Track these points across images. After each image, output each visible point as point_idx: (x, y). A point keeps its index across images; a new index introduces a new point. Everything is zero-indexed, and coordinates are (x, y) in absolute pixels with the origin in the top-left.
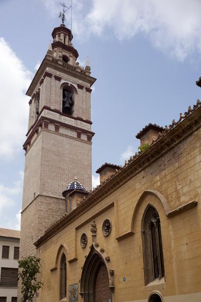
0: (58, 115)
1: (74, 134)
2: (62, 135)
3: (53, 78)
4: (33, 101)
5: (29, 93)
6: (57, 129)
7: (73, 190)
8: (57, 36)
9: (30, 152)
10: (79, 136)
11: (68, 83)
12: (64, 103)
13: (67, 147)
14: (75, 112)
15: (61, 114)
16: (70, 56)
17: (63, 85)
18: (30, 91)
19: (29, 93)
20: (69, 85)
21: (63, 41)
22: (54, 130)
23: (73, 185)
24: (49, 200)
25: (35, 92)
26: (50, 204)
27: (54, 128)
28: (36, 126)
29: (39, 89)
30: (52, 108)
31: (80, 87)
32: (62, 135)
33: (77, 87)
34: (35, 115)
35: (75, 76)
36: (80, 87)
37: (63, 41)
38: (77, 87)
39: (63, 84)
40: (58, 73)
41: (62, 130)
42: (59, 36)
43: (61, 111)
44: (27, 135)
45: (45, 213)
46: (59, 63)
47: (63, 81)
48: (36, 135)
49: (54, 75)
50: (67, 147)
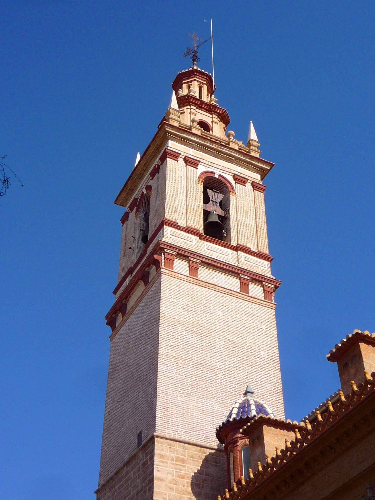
0: (195, 238)
1: (234, 283)
2: (207, 285)
3: (181, 160)
4: (132, 215)
5: (120, 200)
6: (193, 270)
7: (248, 419)
8: (184, 86)
9: (124, 329)
10: (244, 287)
11: (214, 173)
12: (207, 214)
13: (219, 312)
14: (233, 234)
15: (201, 237)
16: (212, 122)
17: (203, 177)
18: (124, 194)
19: (120, 200)
20: (217, 176)
21: (197, 95)
22: (187, 273)
23: (245, 407)
24: (180, 449)
25: (136, 195)
26: (183, 461)
27: (188, 269)
28: (143, 266)
29: (149, 188)
30: (182, 223)
31: (241, 180)
32: (207, 285)
33: (233, 182)
34: (138, 243)
35: (228, 158)
36: (241, 180)
37: (197, 95)
38: (233, 182)
39: (203, 173)
40: (191, 152)
41: (204, 273)
42: (189, 87)
43: (202, 231)
44: (115, 292)
45: (171, 489)
46: (194, 131)
47: (201, 169)
48: (141, 287)
49: (183, 155)
50: (219, 312)
